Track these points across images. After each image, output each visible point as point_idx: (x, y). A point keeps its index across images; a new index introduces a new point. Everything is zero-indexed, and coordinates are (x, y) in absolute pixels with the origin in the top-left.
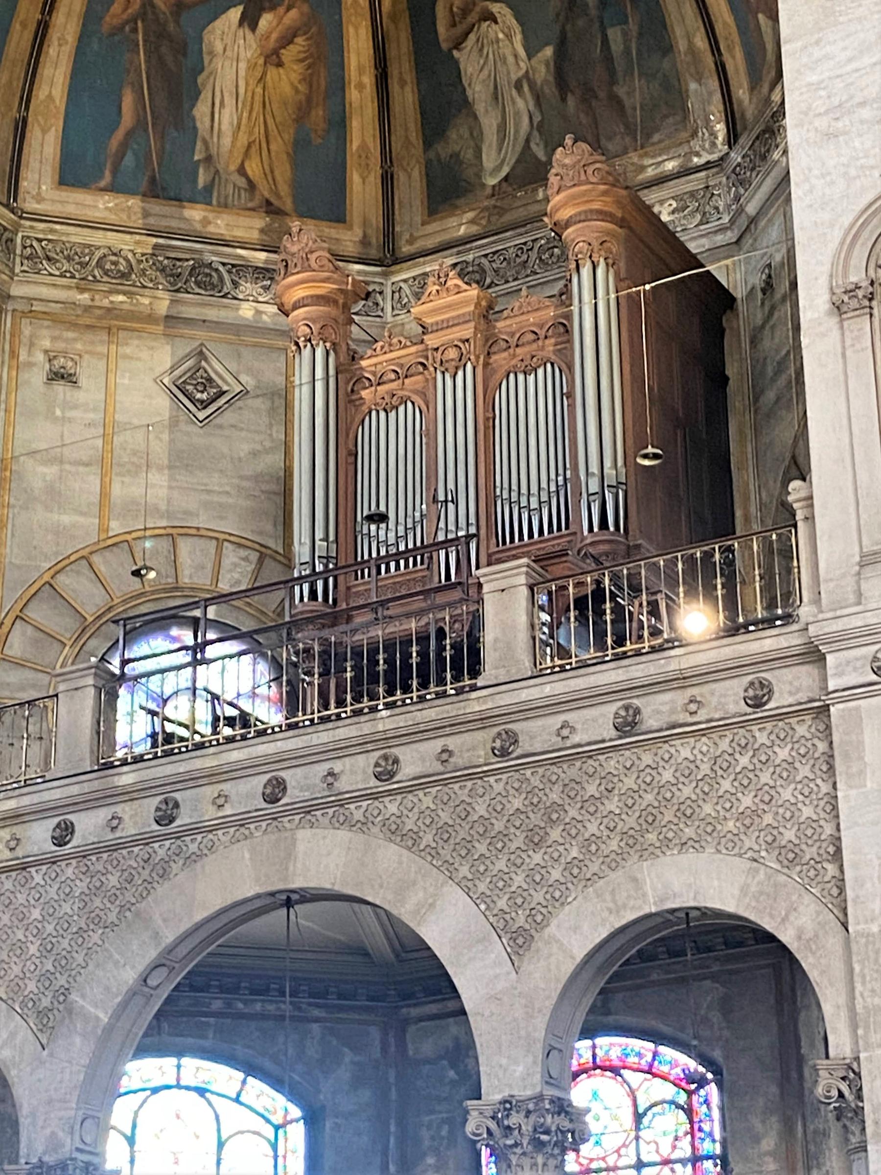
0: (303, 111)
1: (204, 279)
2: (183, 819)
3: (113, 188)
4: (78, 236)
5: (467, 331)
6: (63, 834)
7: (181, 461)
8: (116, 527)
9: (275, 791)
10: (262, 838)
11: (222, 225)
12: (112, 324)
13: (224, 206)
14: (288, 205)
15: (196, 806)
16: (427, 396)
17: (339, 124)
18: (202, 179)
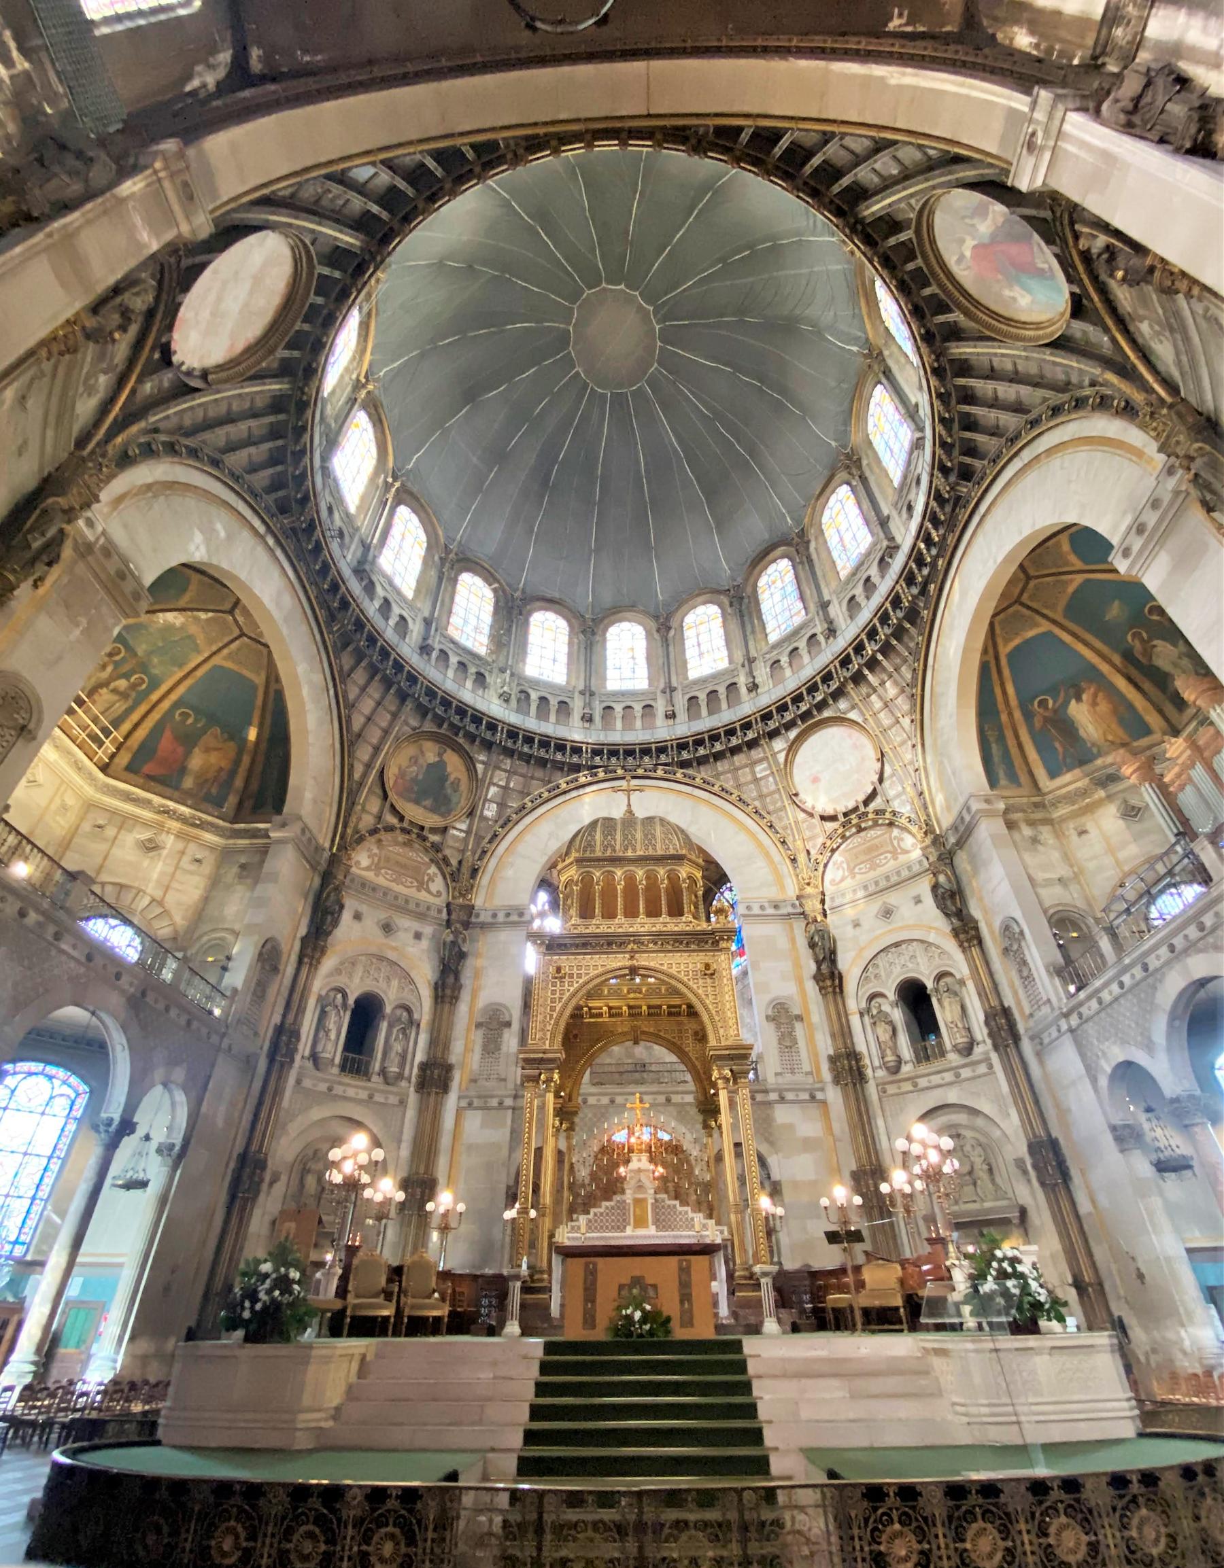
0: (1115, 712)
1: (1113, 778)
2: (1151, 968)
3: (1069, 770)
4: (1064, 791)
5: (1188, 752)
6: (1121, 985)
7: (1137, 837)
8: (1126, 868)
9: (1172, 948)
10: (1178, 967)
11: (1109, 759)
12: (1090, 809)
13: (1107, 753)
14: (1127, 739)
15: (1153, 963)
16: (1190, 779)
17: (1130, 706)
18: (1095, 750)
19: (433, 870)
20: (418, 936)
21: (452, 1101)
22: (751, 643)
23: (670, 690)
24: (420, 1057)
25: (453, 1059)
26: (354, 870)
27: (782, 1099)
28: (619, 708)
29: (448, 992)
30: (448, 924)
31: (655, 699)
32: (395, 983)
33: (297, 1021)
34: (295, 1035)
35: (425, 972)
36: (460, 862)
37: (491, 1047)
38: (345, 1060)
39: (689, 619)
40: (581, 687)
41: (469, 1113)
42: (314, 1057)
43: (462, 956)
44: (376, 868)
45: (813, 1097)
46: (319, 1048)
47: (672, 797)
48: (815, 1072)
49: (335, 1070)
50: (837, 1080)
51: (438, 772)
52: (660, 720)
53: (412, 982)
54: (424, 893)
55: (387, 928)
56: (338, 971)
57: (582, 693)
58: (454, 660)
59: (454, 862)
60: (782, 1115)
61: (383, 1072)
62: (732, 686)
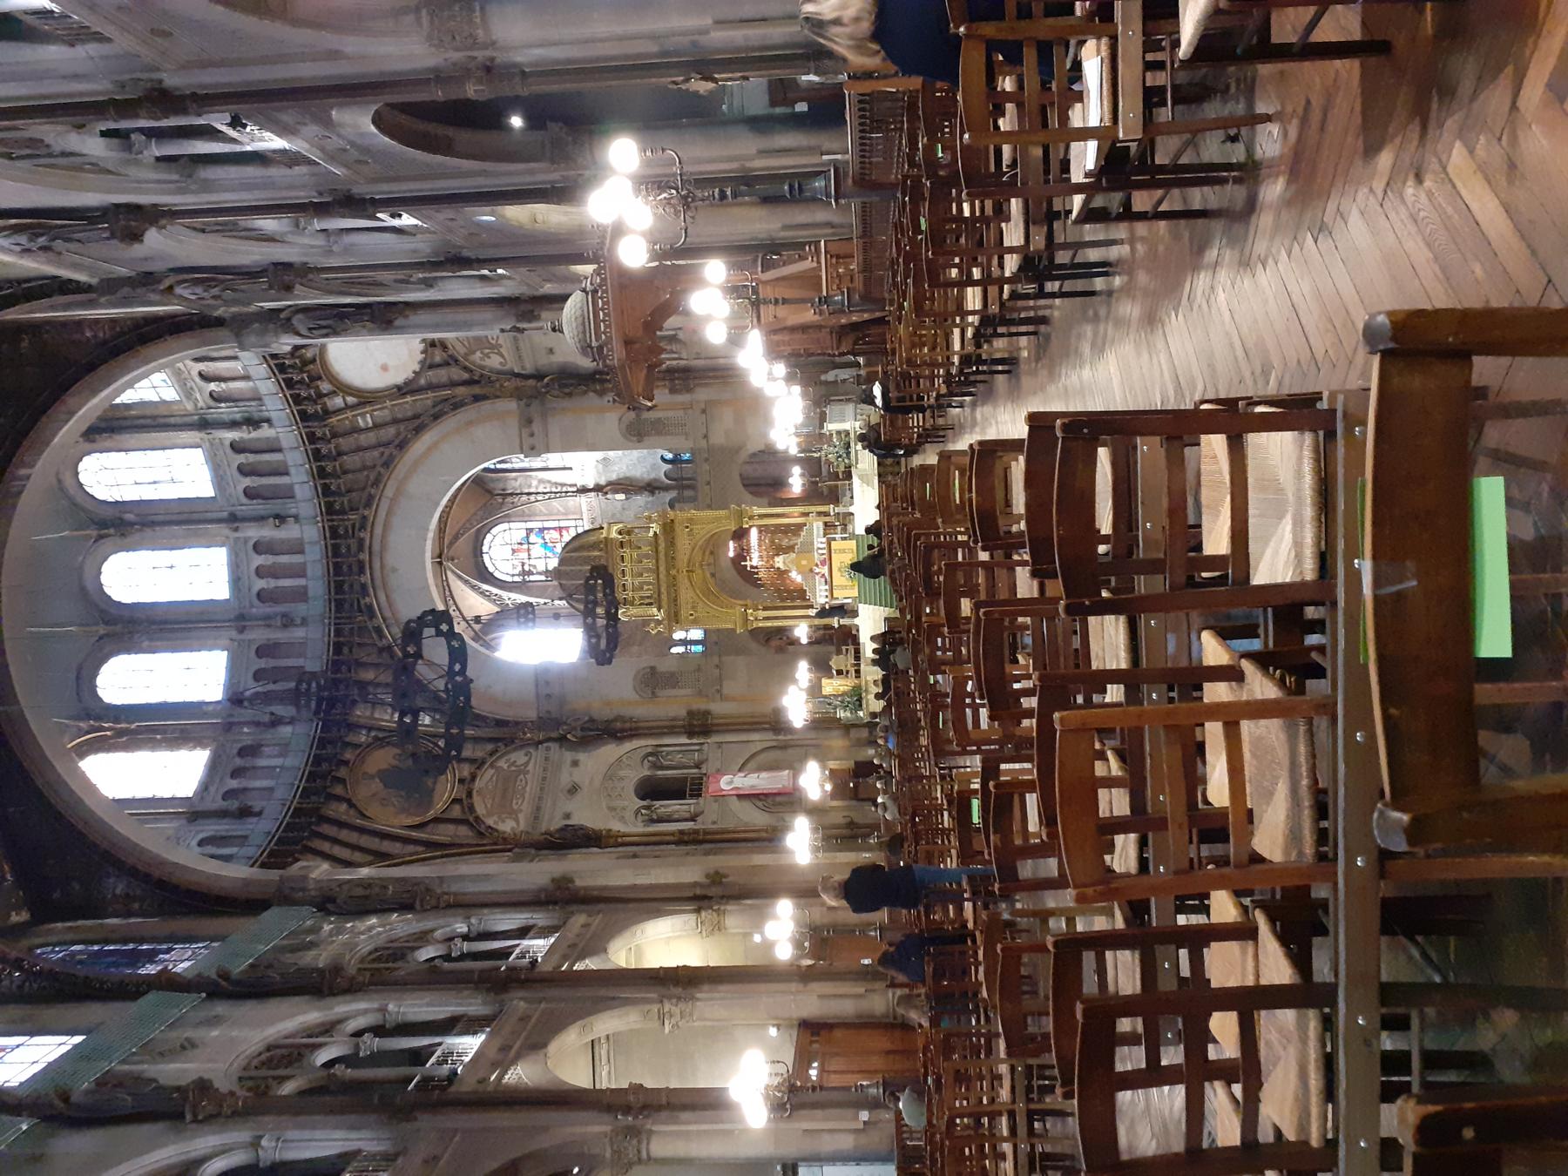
19: (502, 764)
20: (575, 763)
21: (718, 708)
22: (172, 420)
23: (233, 519)
24: (684, 740)
25: (683, 713)
26: (522, 826)
27: (706, 436)
28: (260, 584)
29: (628, 725)
30: (562, 740)
31: (246, 540)
32: (622, 773)
33: (672, 834)
34: (681, 832)
35: (610, 752)
36: (490, 740)
37: (672, 680)
38: (692, 796)
39: (101, 493)
40: (234, 634)
41: (725, 691)
42: (693, 819)
43: (592, 720)
44: (513, 814)
45: (704, 411)
46: (687, 815)
47: (396, 521)
48: (687, 407)
49: (701, 800)
50: (689, 390)
51: (390, 778)
52: (290, 532)
53: (619, 760)
54: (530, 767)
55: (573, 790)
56: (622, 819)
57: (241, 630)
58: (234, 784)
59: (490, 747)
60: (718, 438)
61: (698, 766)
62: (236, 448)
